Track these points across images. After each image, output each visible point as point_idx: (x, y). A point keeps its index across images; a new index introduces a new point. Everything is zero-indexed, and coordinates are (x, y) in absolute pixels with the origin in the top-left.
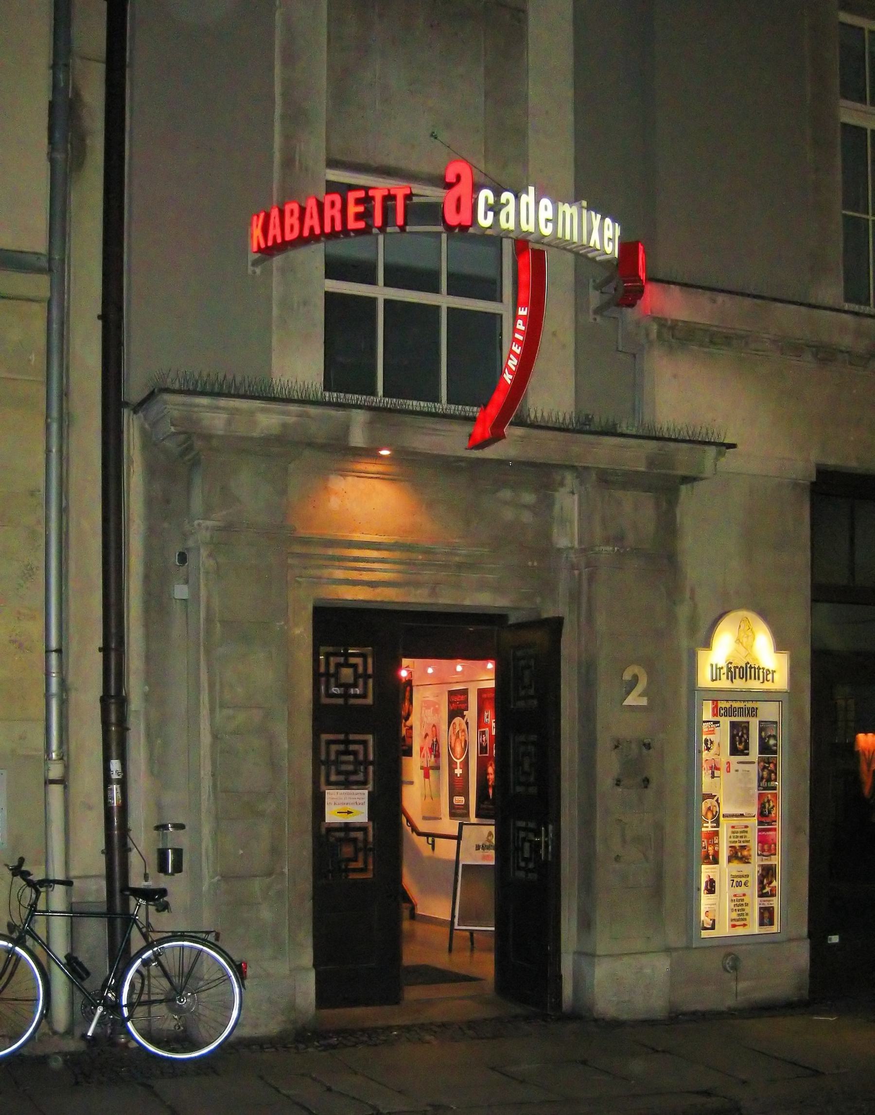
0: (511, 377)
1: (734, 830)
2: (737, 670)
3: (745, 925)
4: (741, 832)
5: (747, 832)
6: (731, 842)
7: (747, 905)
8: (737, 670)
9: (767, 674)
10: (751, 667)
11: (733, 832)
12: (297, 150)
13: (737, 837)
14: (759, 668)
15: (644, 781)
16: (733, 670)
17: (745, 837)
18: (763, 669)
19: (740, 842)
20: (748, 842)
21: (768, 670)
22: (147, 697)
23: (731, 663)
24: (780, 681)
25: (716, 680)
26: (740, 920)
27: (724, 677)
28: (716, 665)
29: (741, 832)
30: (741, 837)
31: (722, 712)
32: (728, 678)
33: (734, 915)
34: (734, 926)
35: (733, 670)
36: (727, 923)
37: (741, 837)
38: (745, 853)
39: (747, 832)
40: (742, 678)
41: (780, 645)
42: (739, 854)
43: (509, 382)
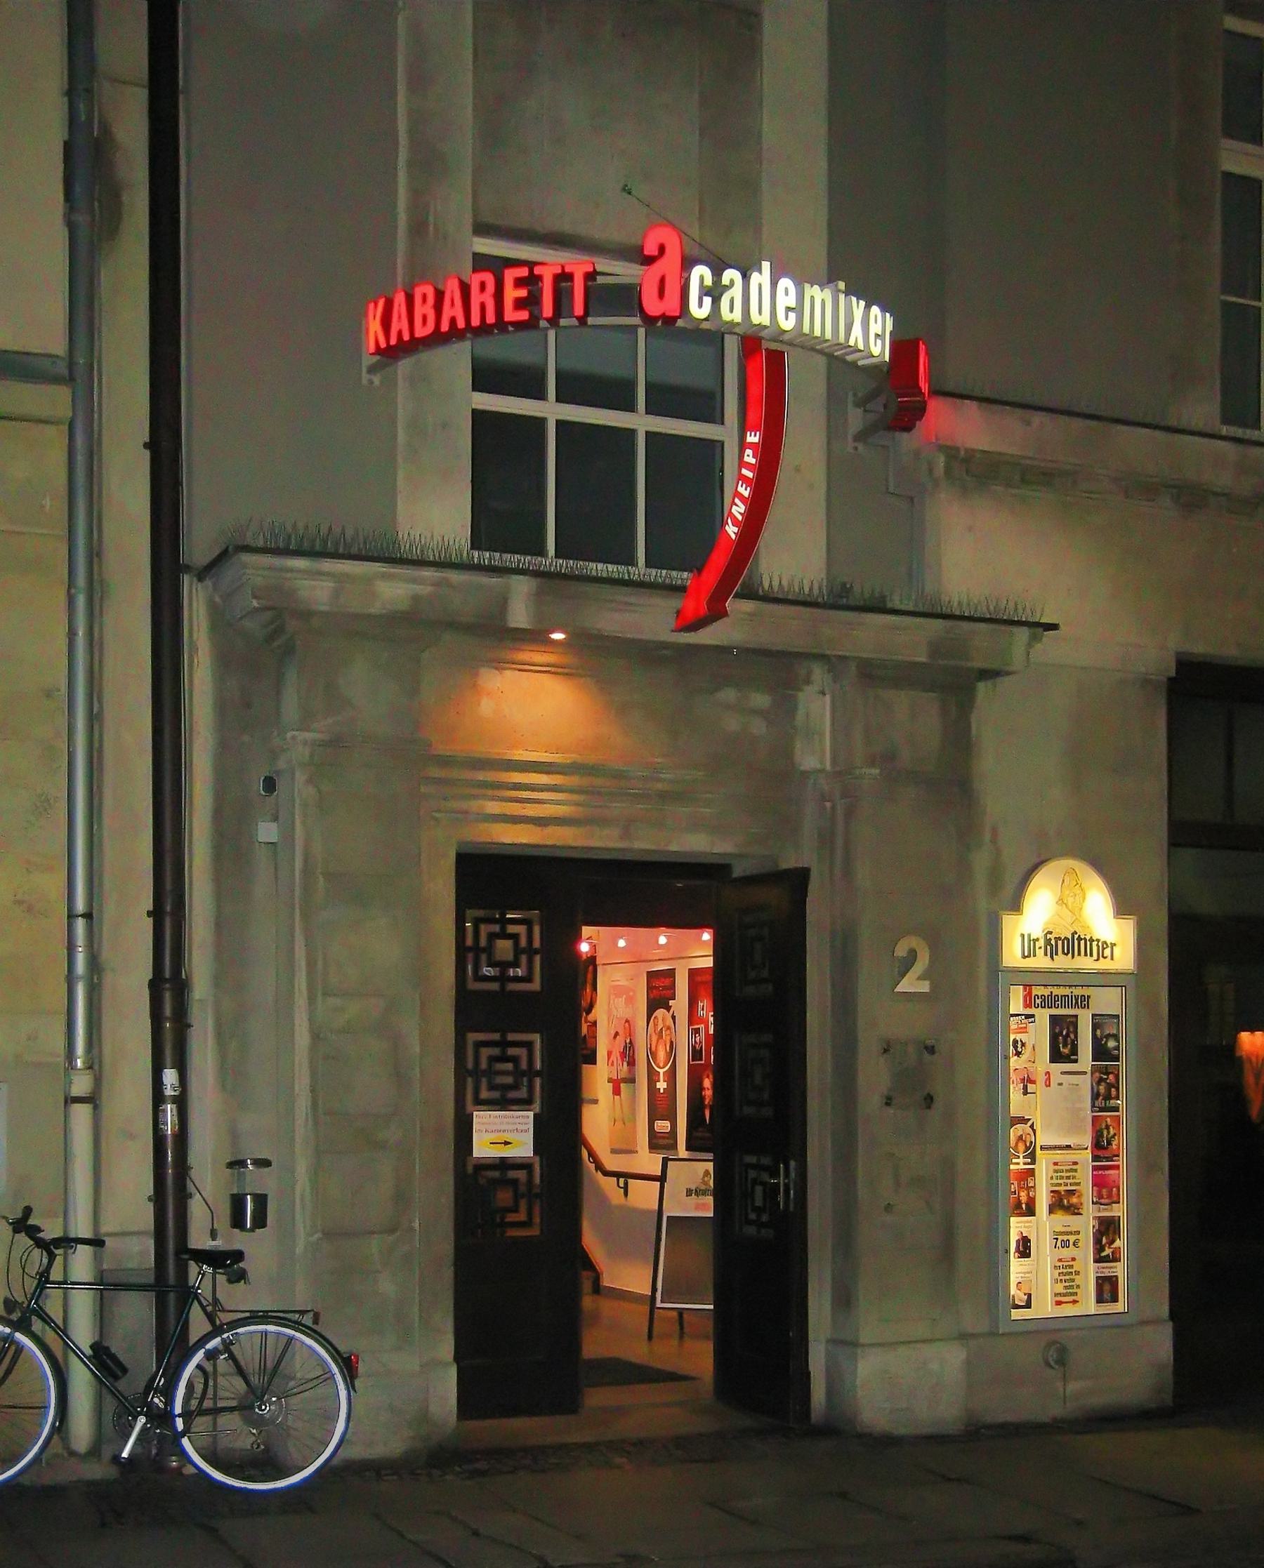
2: (1060, 943)
3: (1075, 1302)
4: (1067, 1171)
5: (1076, 1171)
6: (1052, 1185)
7: (1077, 1273)
8: (1060, 943)
10: (1079, 939)
11: (1056, 1171)
13: (1062, 1178)
14: (1092, 940)
16: (1053, 942)
17: (1074, 1177)
18: (1098, 941)
20: (1079, 1184)
23: (1051, 933)
24: (1123, 958)
25: (1029, 956)
26: (1068, 1295)
27: (1040, 953)
28: (1029, 935)
29: (1067, 1171)
30: (1068, 1178)
31: (1038, 1001)
33: (1060, 1288)
34: (1059, 1303)
35: (1053, 942)
36: (1049, 1299)
37: (1068, 1178)
38: (1074, 1200)
39: (1076, 1171)
41: (1122, 909)
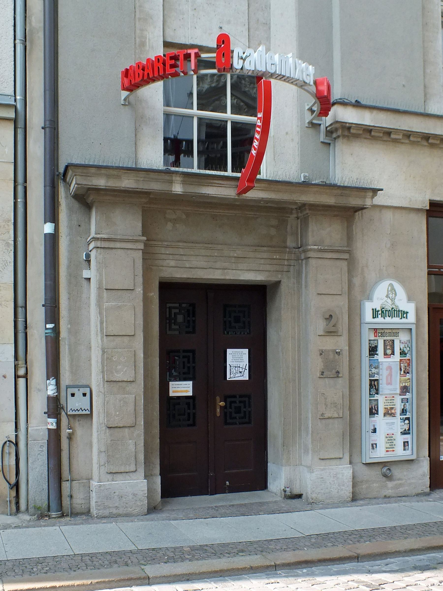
0: (255, 152)
1: (386, 399)
2: (387, 312)
3: (393, 451)
4: (390, 400)
5: (394, 400)
6: (385, 405)
7: (394, 440)
8: (387, 312)
9: (404, 314)
10: (394, 310)
11: (386, 400)
12: (148, 38)
13: (388, 402)
14: (399, 311)
15: (336, 373)
16: (384, 312)
17: (393, 402)
18: (401, 311)
19: (390, 405)
20: (395, 405)
21: (404, 312)
22: (69, 331)
23: (383, 308)
24: (411, 318)
25: (376, 317)
26: (391, 447)
27: (380, 316)
28: (376, 309)
29: (390, 400)
30: (391, 403)
31: (380, 335)
32: (382, 317)
33: (388, 446)
34: (387, 451)
35: (384, 312)
36: (384, 450)
37: (391, 403)
38: (393, 411)
39: (394, 400)
40: (390, 317)
41: (410, 299)
42: (390, 412)
43: (254, 154)
